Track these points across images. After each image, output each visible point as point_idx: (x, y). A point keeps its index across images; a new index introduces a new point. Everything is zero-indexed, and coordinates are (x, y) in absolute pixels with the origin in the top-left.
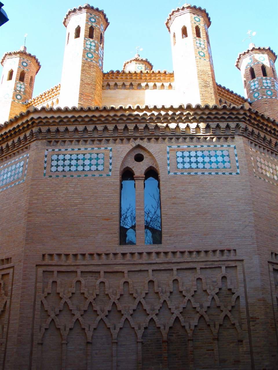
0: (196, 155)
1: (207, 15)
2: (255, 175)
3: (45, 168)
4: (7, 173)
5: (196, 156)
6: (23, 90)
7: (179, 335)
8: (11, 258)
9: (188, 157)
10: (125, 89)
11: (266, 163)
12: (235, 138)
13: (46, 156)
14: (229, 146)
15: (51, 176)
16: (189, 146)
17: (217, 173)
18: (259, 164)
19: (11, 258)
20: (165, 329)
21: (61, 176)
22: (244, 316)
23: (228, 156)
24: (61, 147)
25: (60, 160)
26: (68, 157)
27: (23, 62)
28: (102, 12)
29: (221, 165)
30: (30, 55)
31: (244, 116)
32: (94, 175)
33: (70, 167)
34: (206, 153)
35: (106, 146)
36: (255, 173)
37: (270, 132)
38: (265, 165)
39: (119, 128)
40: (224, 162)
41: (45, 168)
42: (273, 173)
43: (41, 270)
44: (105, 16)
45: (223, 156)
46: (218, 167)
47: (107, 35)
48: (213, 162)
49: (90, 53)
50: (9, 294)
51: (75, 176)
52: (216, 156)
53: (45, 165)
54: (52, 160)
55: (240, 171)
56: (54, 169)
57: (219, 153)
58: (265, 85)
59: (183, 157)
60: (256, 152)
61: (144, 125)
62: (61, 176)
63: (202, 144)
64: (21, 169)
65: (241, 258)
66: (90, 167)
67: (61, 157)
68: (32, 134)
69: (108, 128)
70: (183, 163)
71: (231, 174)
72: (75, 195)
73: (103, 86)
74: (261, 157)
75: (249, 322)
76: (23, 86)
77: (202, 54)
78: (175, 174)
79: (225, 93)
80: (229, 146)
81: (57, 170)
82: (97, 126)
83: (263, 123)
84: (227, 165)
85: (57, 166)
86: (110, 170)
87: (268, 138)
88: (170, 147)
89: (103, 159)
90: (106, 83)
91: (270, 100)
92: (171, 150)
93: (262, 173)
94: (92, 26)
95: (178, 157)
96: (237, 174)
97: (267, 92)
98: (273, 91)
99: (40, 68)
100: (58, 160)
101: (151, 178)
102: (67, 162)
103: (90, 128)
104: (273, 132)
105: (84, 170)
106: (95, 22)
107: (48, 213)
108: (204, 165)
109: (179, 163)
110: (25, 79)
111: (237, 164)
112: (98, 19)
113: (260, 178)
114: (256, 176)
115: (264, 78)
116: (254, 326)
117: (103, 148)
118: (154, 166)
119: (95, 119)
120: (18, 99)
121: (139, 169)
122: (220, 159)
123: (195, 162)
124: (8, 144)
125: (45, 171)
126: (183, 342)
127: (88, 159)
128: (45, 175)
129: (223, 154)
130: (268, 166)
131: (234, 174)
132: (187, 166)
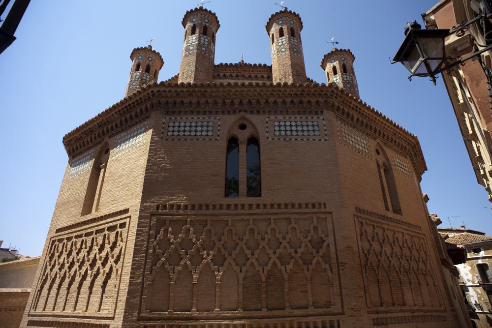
1: (300, 19)
3: (163, 133)
5: (291, 126)
7: (276, 277)
8: (128, 209)
9: (284, 126)
14: (318, 118)
15: (167, 140)
16: (285, 118)
17: (308, 140)
19: (128, 209)
20: (263, 272)
21: (176, 140)
22: (334, 261)
23: (318, 126)
24: (177, 116)
26: (182, 124)
27: (149, 57)
29: (311, 133)
30: (154, 51)
31: (332, 93)
32: (205, 139)
34: (299, 123)
35: (215, 116)
37: (353, 109)
41: (163, 133)
44: (216, 18)
45: (313, 126)
46: (309, 135)
47: (217, 35)
49: (203, 47)
50: (125, 240)
51: (188, 140)
52: (308, 126)
53: (163, 130)
55: (328, 138)
56: (170, 134)
57: (310, 123)
58: (345, 79)
59: (280, 126)
60: (341, 124)
61: (247, 100)
62: (176, 140)
63: (295, 116)
65: (330, 211)
66: (201, 132)
67: (177, 124)
68: (152, 106)
69: (218, 101)
71: (320, 140)
73: (214, 76)
75: (338, 267)
76: (148, 77)
78: (273, 139)
80: (318, 118)
82: (208, 100)
84: (317, 133)
85: (173, 131)
86: (218, 136)
87: (351, 112)
89: (212, 126)
90: (217, 74)
92: (269, 120)
93: (346, 141)
96: (326, 140)
98: (351, 84)
99: (163, 64)
100: (174, 127)
102: (182, 129)
103: (203, 101)
108: (297, 132)
110: (150, 71)
111: (326, 133)
113: (345, 145)
114: (341, 143)
115: (345, 74)
116: (343, 270)
117: (212, 118)
118: (255, 133)
119: (206, 94)
122: (311, 128)
123: (290, 131)
124: (131, 114)
125: (162, 135)
131: (323, 140)
132: (283, 133)
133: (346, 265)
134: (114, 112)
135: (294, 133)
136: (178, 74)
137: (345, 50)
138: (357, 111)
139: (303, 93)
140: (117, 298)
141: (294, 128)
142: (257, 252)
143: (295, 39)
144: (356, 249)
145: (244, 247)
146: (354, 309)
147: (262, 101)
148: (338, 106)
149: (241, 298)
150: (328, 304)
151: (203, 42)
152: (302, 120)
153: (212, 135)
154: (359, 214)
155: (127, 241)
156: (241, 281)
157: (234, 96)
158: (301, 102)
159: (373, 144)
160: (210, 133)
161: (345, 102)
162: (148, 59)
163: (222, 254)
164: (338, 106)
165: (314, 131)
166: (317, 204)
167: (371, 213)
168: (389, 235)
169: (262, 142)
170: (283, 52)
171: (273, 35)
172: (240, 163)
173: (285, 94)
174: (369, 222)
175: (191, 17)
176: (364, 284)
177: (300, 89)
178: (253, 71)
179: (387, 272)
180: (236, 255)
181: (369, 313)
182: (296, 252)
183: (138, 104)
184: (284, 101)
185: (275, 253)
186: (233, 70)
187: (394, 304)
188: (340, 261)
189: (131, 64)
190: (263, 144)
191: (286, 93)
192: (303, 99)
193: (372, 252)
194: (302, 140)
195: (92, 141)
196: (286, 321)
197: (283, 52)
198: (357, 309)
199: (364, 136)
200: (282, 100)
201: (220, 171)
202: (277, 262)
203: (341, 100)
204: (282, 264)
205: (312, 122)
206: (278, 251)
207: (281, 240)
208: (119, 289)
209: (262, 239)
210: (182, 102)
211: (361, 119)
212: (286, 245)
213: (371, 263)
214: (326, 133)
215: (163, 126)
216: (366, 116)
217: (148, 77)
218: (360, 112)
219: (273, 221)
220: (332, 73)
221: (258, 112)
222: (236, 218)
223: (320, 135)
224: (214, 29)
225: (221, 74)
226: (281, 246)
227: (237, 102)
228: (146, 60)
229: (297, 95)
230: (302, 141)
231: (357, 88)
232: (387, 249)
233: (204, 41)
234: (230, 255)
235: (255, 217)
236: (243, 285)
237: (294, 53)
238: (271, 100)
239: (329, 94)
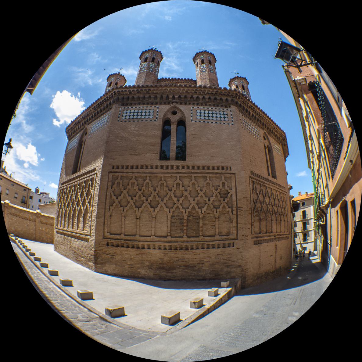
3: (119, 117)
7: (194, 217)
13: (120, 111)
15: (121, 122)
20: (185, 213)
21: (127, 121)
23: (227, 114)
24: (129, 106)
32: (147, 121)
34: (214, 112)
35: (155, 105)
39: (163, 96)
41: (119, 117)
43: (111, 175)
44: (161, 54)
45: (224, 114)
54: (123, 113)
56: (124, 118)
57: (222, 113)
59: (200, 113)
62: (127, 121)
68: (114, 102)
70: (201, 116)
75: (237, 210)
77: (212, 71)
80: (227, 110)
84: (226, 119)
85: (126, 116)
86: (157, 118)
87: (249, 109)
88: (193, 107)
89: (153, 112)
96: (232, 124)
100: (127, 113)
102: (132, 114)
103: (147, 96)
105: (141, 118)
107: (118, 142)
111: (232, 120)
116: (240, 212)
117: (153, 107)
121: (174, 119)
122: (222, 116)
125: (119, 119)
128: (118, 121)
131: (230, 124)
132: (203, 118)
133: (242, 209)
134: (91, 109)
135: (211, 118)
138: (252, 109)
139: (217, 93)
140: (91, 224)
141: (211, 115)
142: (181, 199)
145: (172, 195)
147: (189, 96)
150: (228, 234)
151: (151, 65)
154: (252, 176)
155: (95, 189)
156: (169, 218)
157: (169, 93)
158: (215, 99)
159: (262, 132)
160: (151, 117)
163: (157, 200)
165: (224, 118)
166: (225, 167)
167: (260, 176)
168: (269, 191)
171: (197, 63)
173: (205, 93)
177: (215, 90)
179: (265, 213)
180: (166, 201)
181: (252, 238)
182: (209, 200)
183: (105, 101)
185: (194, 200)
187: (266, 233)
188: (238, 206)
190: (188, 124)
191: (205, 92)
192: (217, 97)
193: (258, 201)
194: (216, 123)
195: (79, 128)
196: (200, 244)
200: (202, 97)
202: (195, 207)
204: (199, 208)
205: (223, 112)
206: (197, 199)
207: (199, 191)
208: (91, 219)
209: (185, 190)
210: (133, 98)
211: (254, 115)
212: (202, 195)
213: (257, 208)
216: (258, 114)
218: (254, 111)
219: (193, 178)
221: (186, 104)
222: (168, 175)
226: (199, 195)
227: (171, 96)
229: (213, 94)
232: (267, 200)
234: (162, 201)
235: (181, 175)
236: (171, 221)
239: (234, 95)
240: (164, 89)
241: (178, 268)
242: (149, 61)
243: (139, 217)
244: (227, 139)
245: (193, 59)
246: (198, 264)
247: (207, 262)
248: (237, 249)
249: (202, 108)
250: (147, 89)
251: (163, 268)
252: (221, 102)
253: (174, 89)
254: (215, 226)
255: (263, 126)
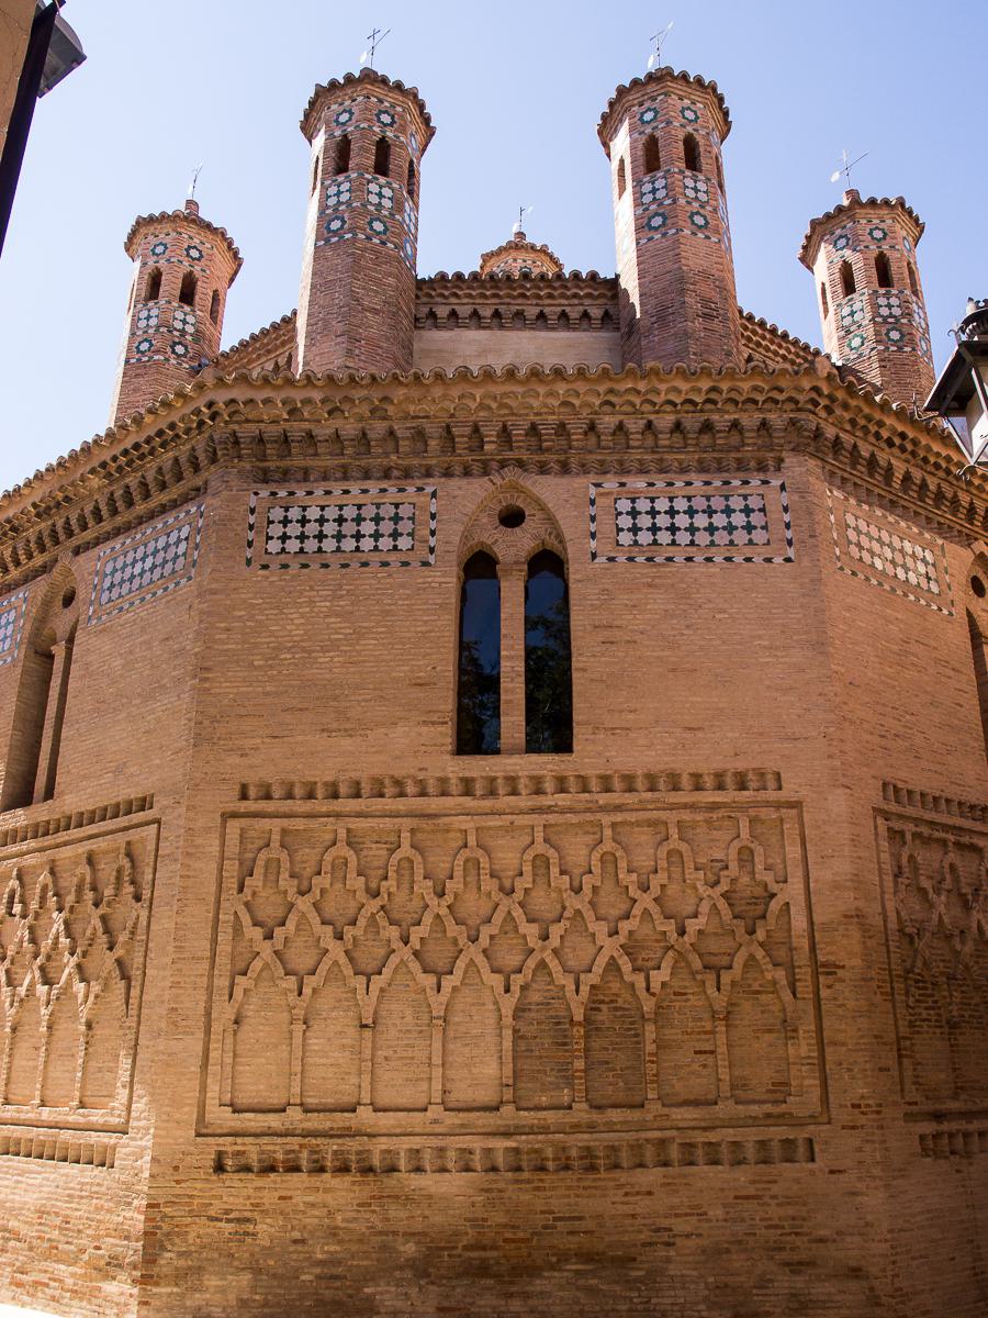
0: (672, 507)
1: (721, 99)
2: (839, 565)
3: (250, 544)
4: (143, 560)
5: (672, 512)
6: (190, 329)
7: (616, 1009)
10: (480, 327)
11: (874, 532)
12: (787, 460)
13: (252, 511)
15: (265, 567)
18: (852, 534)
20: (577, 992)
22: (802, 958)
23: (762, 510)
25: (291, 522)
26: (313, 513)
28: (413, 95)
30: (208, 226)
31: (814, 395)
33: (320, 542)
35: (419, 483)
36: (838, 558)
37: (890, 443)
38: (871, 538)
40: (749, 528)
42: (893, 562)
43: (234, 827)
44: (421, 106)
45: (747, 511)
47: (427, 168)
48: (717, 529)
49: (378, 219)
50: (146, 894)
52: (728, 511)
53: (251, 536)
56: (274, 546)
57: (736, 503)
58: (884, 311)
59: (634, 513)
60: (846, 499)
62: (294, 568)
63: (687, 478)
64: (183, 546)
66: (376, 541)
67: (294, 513)
70: (635, 530)
72: (333, 620)
73: (417, 320)
74: (859, 513)
75: (816, 974)
76: (190, 319)
77: (699, 220)
79: (764, 338)
80: (765, 482)
81: (283, 549)
83: (869, 419)
84: (759, 536)
85: (284, 538)
87: (883, 457)
88: (598, 485)
89: (412, 519)
90: (426, 310)
91: (897, 355)
92: (601, 494)
93: (861, 559)
94: (384, 137)
95: (620, 513)
96: (788, 560)
97: (887, 334)
99: (240, 265)
100: (285, 522)
101: (545, 573)
102: (312, 529)
104: (897, 441)
106: (391, 125)
109: (622, 530)
111: (789, 534)
112: (401, 116)
113: (854, 574)
114: (841, 569)
115: (882, 291)
116: (829, 987)
117: (411, 490)
120: (179, 356)
121: (512, 548)
122: (738, 519)
126: (630, 1029)
127: (371, 520)
129: (746, 505)
130: (879, 540)
131: (778, 560)
133: (840, 973)
135: (683, 538)
136: (295, 313)
137: (886, 202)
138: (903, 449)
139: (713, 396)
141: (682, 521)
142: (556, 931)
143: (701, 177)
144: (879, 921)
145: (518, 913)
146: (859, 1106)
148: (837, 437)
149: (508, 1070)
150: (781, 1090)
152: (709, 490)
153: (412, 549)
154: (893, 807)
156: (508, 1021)
157: (482, 414)
158: (707, 427)
160: (404, 543)
161: (862, 422)
162: (188, 255)
163: (449, 934)
164: (837, 437)
165: (749, 528)
169: (576, 572)
170: (656, 229)
172: (503, 642)
173: (654, 404)
174: (925, 830)
175: (334, 107)
176: (897, 1033)
178: (550, 296)
180: (492, 937)
181: (909, 1117)
182: (682, 932)
183: (163, 445)
184: (649, 425)
185: (614, 933)
186: (485, 297)
188: (821, 958)
189: (130, 273)
190: (578, 577)
192: (715, 417)
194: (709, 560)
195: (17, 563)
196: (647, 1140)
197: (656, 229)
198: (868, 1106)
199: (927, 536)
200: (642, 423)
201: (439, 668)
202: (620, 962)
203: (847, 416)
204: (636, 969)
205: (745, 497)
206: (625, 926)
207: (634, 892)
209: (572, 889)
211: (917, 475)
212: (648, 907)
214: (789, 534)
215: (252, 519)
216: (937, 466)
217: (190, 319)
219: (608, 832)
220: (839, 289)
221: (565, 469)
222: (494, 822)
223: (768, 543)
224: (414, 144)
225: (442, 311)
226: (634, 912)
228: (178, 262)
230: (710, 564)
231: (928, 341)
233: (380, 195)
234: (474, 940)
235: (552, 818)
236: (515, 1031)
237: (694, 234)
238: (608, 421)
240: (455, 392)
241: (553, 1268)
242: (361, 169)
243: (370, 1021)
244: (760, 637)
245: (600, 133)
246: (644, 1245)
247: (688, 1236)
248: (832, 1172)
249: (639, 483)
250: (376, 395)
251: (483, 1270)
252: (735, 440)
253: (506, 394)
254: (712, 1052)
255: (971, 520)
